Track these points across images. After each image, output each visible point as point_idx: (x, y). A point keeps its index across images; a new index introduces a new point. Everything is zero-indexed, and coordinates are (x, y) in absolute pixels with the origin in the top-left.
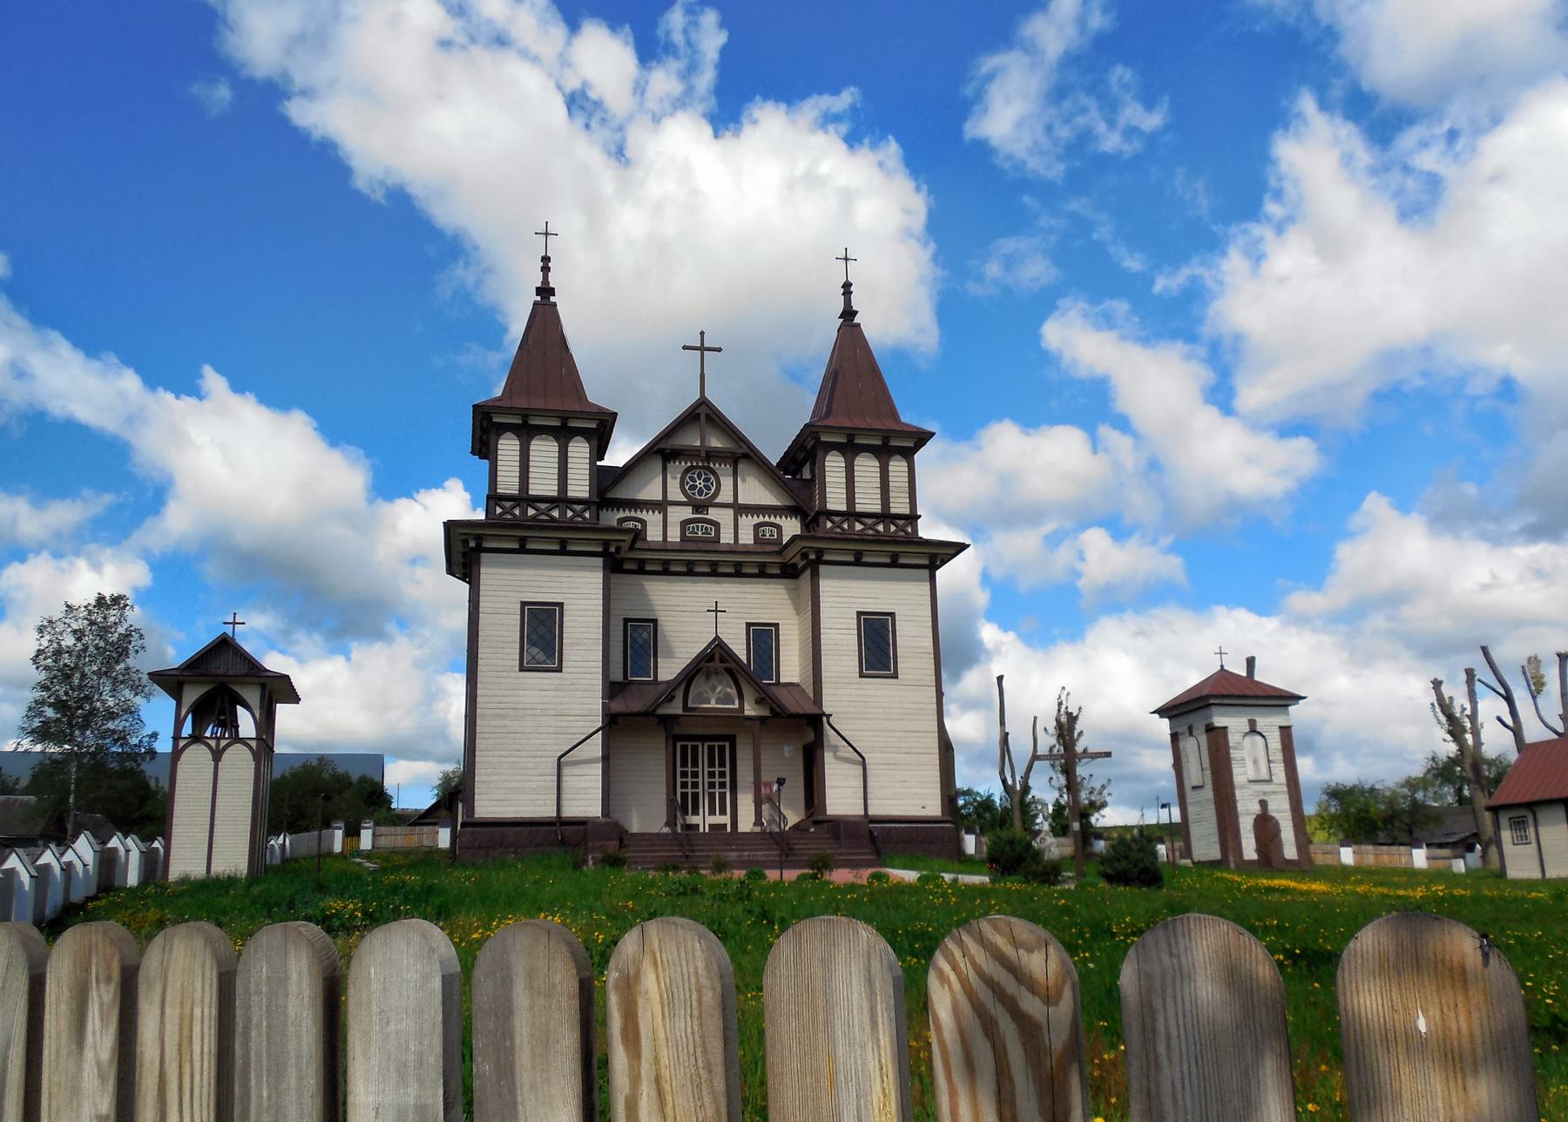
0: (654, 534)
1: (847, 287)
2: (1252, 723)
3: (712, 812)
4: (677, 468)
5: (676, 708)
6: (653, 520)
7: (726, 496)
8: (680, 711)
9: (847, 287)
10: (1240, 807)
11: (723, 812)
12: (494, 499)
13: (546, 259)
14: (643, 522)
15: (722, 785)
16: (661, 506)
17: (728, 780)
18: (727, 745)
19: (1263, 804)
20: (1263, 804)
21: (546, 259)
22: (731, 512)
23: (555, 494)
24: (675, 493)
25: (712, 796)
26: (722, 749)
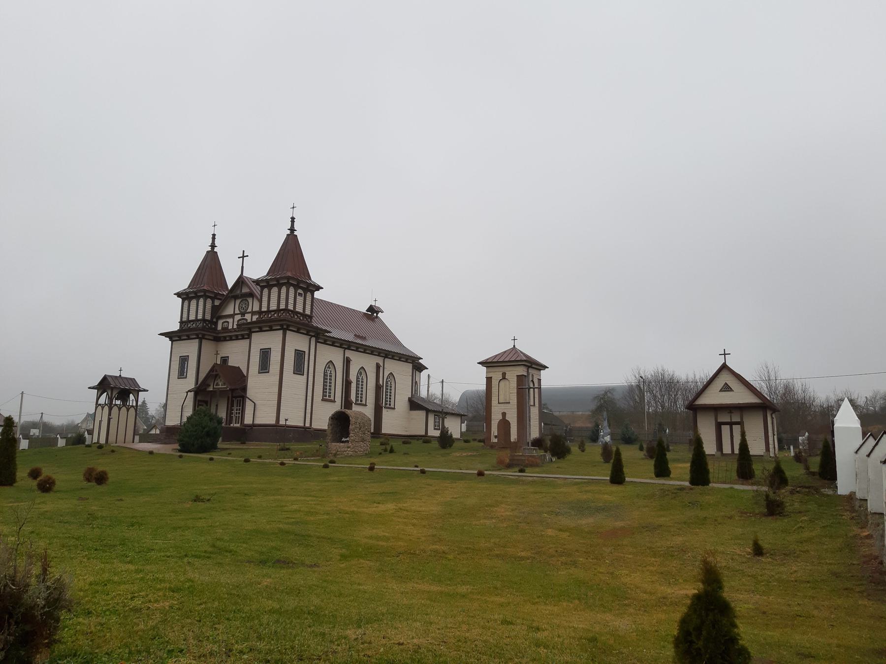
0: (230, 327)
1: (293, 219)
2: (504, 375)
3: (236, 423)
4: (238, 302)
5: (211, 389)
6: (230, 320)
7: (249, 310)
8: (212, 389)
9: (293, 219)
10: (493, 417)
11: (238, 423)
12: (181, 322)
13: (214, 235)
14: (228, 322)
15: (239, 414)
16: (232, 316)
17: (240, 411)
18: (242, 399)
19: (504, 414)
20: (504, 414)
21: (214, 235)
22: (250, 315)
23: (194, 319)
24: (237, 311)
25: (236, 417)
26: (240, 400)
